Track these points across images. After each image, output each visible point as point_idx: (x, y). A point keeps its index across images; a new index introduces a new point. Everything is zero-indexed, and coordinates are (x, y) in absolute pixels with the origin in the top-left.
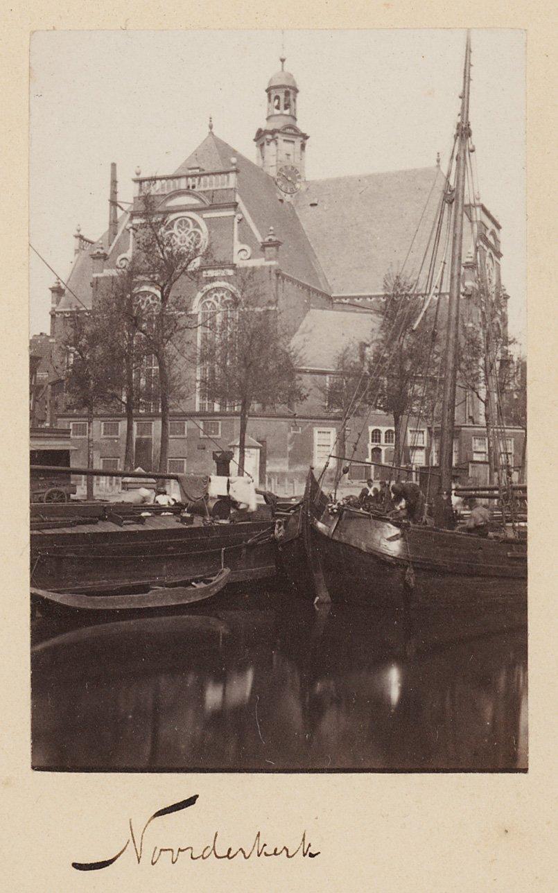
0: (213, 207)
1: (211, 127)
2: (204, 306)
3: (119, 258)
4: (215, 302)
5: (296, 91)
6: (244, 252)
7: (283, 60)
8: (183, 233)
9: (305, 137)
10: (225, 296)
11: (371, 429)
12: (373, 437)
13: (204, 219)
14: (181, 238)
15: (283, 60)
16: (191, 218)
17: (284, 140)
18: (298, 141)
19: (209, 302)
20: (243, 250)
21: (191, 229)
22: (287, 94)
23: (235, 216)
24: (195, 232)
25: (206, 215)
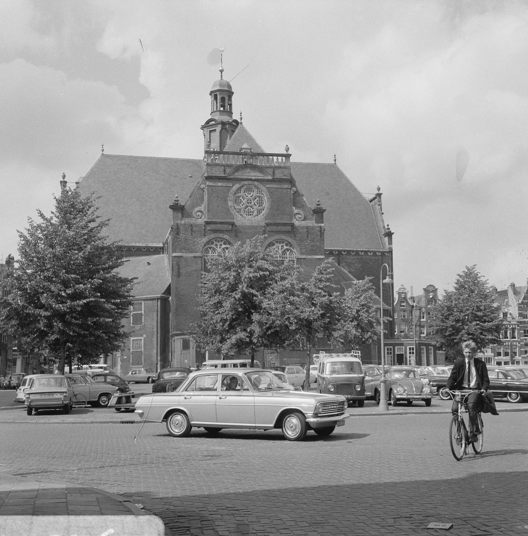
0: (273, 181)
3: (197, 209)
6: (300, 216)
7: (221, 71)
8: (249, 196)
15: (221, 71)
16: (255, 186)
23: (291, 189)
24: (259, 197)
25: (268, 186)
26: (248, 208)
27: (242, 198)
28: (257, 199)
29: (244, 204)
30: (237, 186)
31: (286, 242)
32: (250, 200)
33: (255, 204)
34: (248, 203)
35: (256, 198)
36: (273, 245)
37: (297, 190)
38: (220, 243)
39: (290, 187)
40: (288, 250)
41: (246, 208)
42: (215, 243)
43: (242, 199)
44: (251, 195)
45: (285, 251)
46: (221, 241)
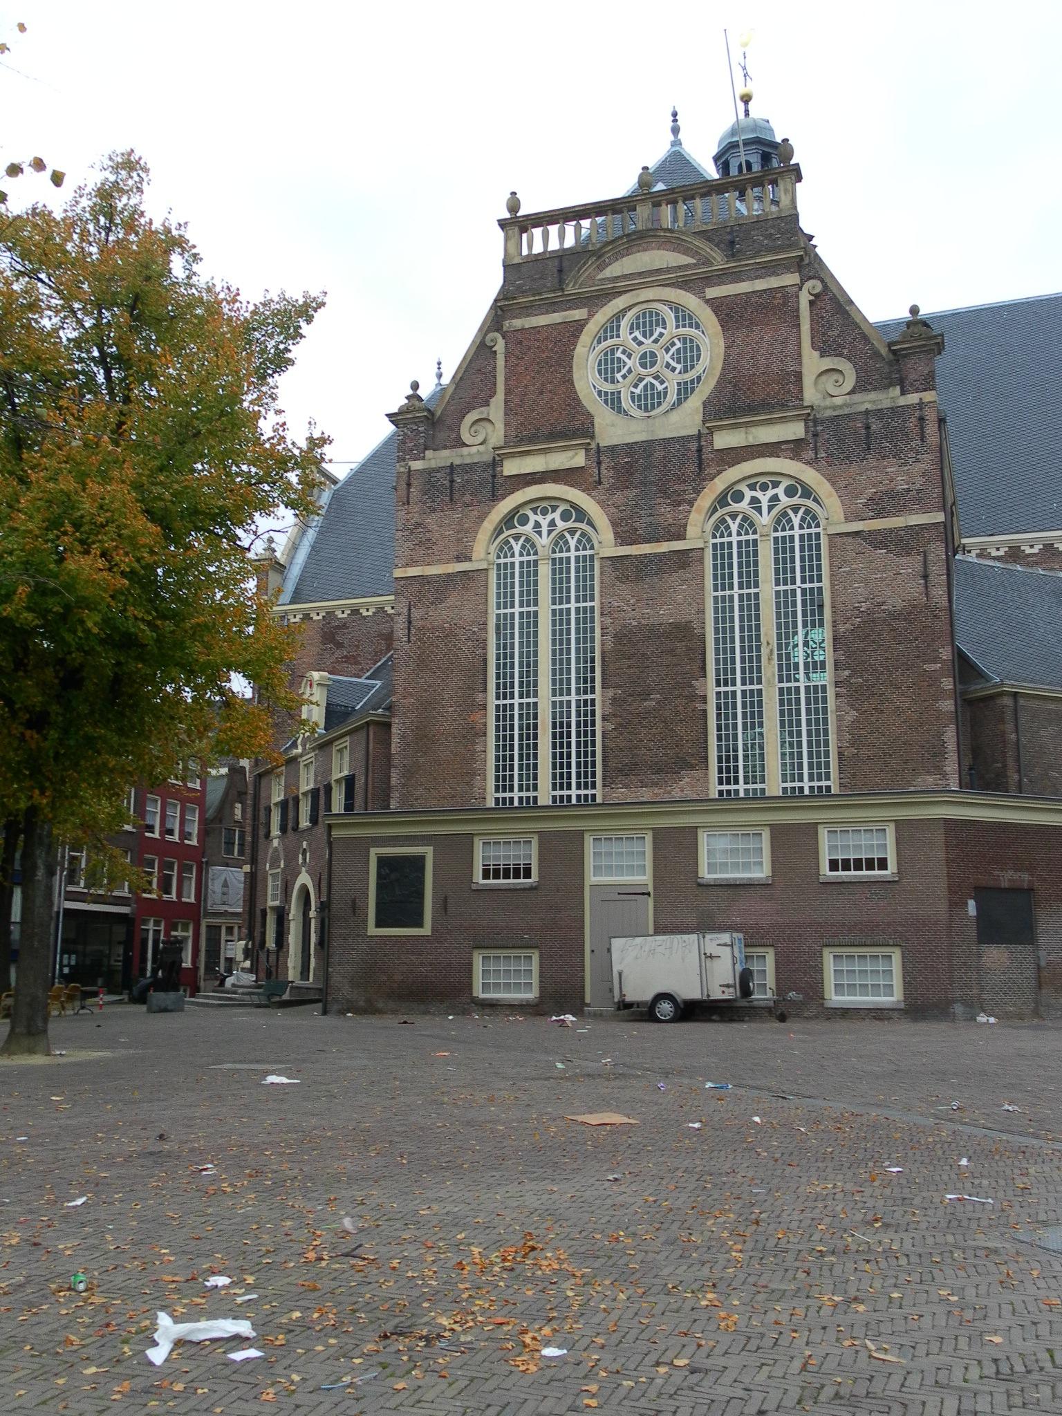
1: (675, 130)
2: (721, 527)
4: (753, 514)
6: (836, 376)
7: (746, 99)
8: (648, 342)
10: (782, 496)
13: (707, 301)
14: (644, 356)
19: (734, 516)
20: (840, 372)
21: (671, 329)
24: (684, 339)
25: (712, 292)
26: (641, 385)
27: (624, 352)
28: (679, 345)
29: (630, 371)
30: (603, 315)
31: (785, 483)
32: (653, 355)
33: (668, 365)
34: (644, 366)
35: (673, 344)
36: (739, 497)
37: (825, 287)
38: (549, 517)
39: (798, 282)
40: (796, 509)
41: (636, 386)
42: (533, 518)
43: (624, 357)
44: (653, 338)
45: (784, 514)
46: (554, 508)
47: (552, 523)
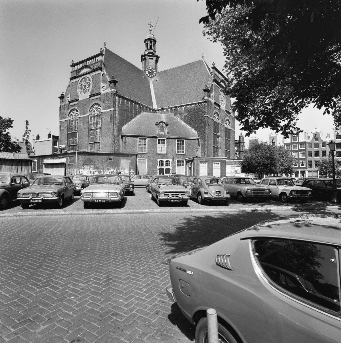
5: (155, 42)
6: (104, 88)
9: (158, 57)
11: (159, 160)
12: (160, 163)
16: (88, 77)
17: (149, 58)
18: (155, 58)
22: (151, 42)
47: (75, 112)
